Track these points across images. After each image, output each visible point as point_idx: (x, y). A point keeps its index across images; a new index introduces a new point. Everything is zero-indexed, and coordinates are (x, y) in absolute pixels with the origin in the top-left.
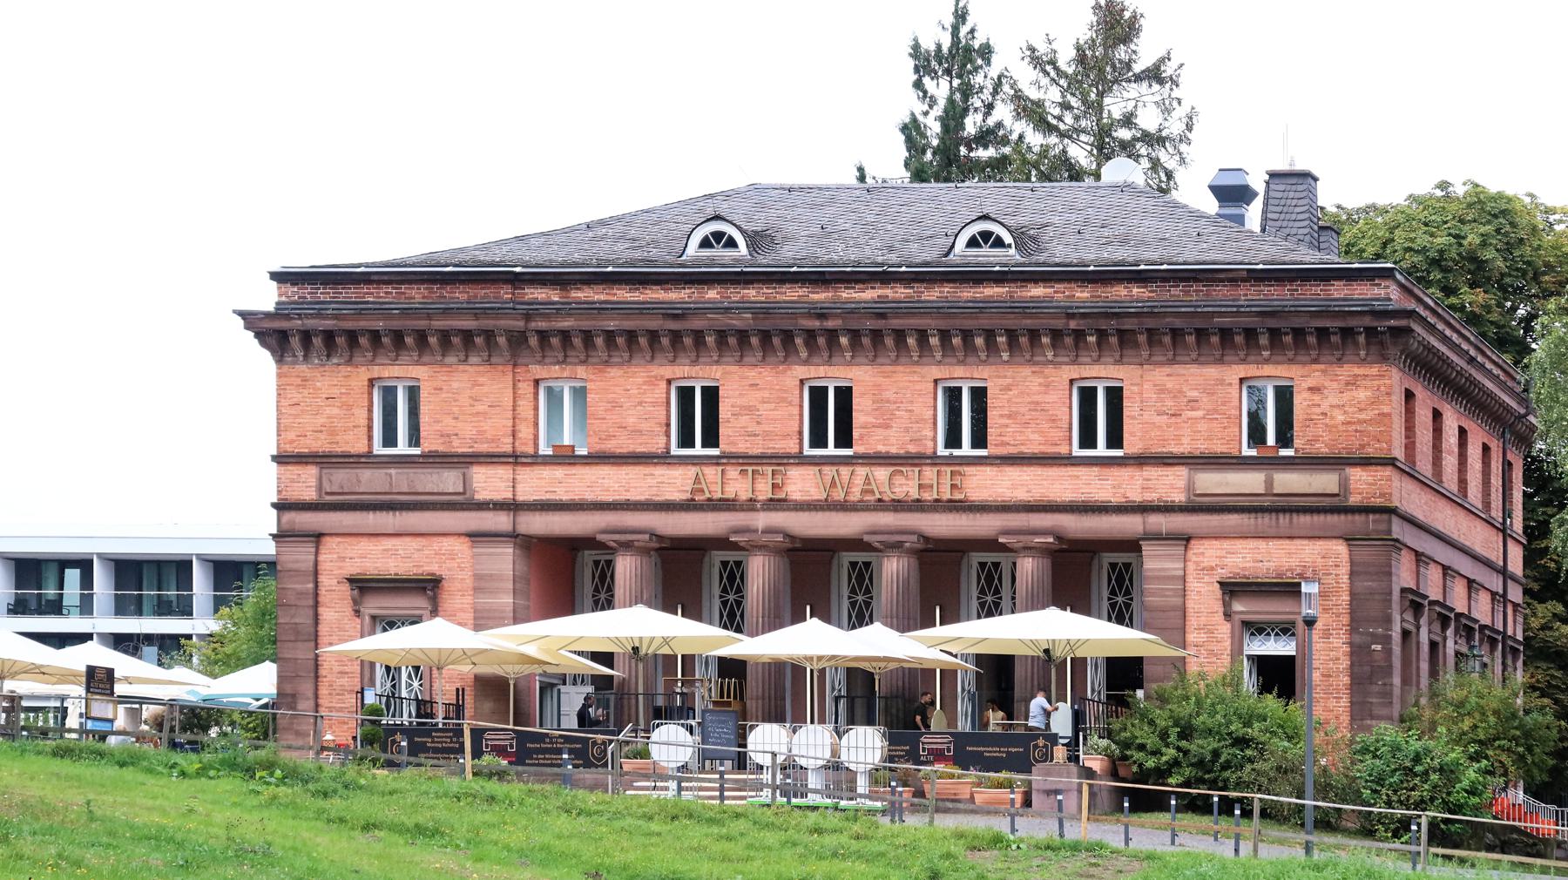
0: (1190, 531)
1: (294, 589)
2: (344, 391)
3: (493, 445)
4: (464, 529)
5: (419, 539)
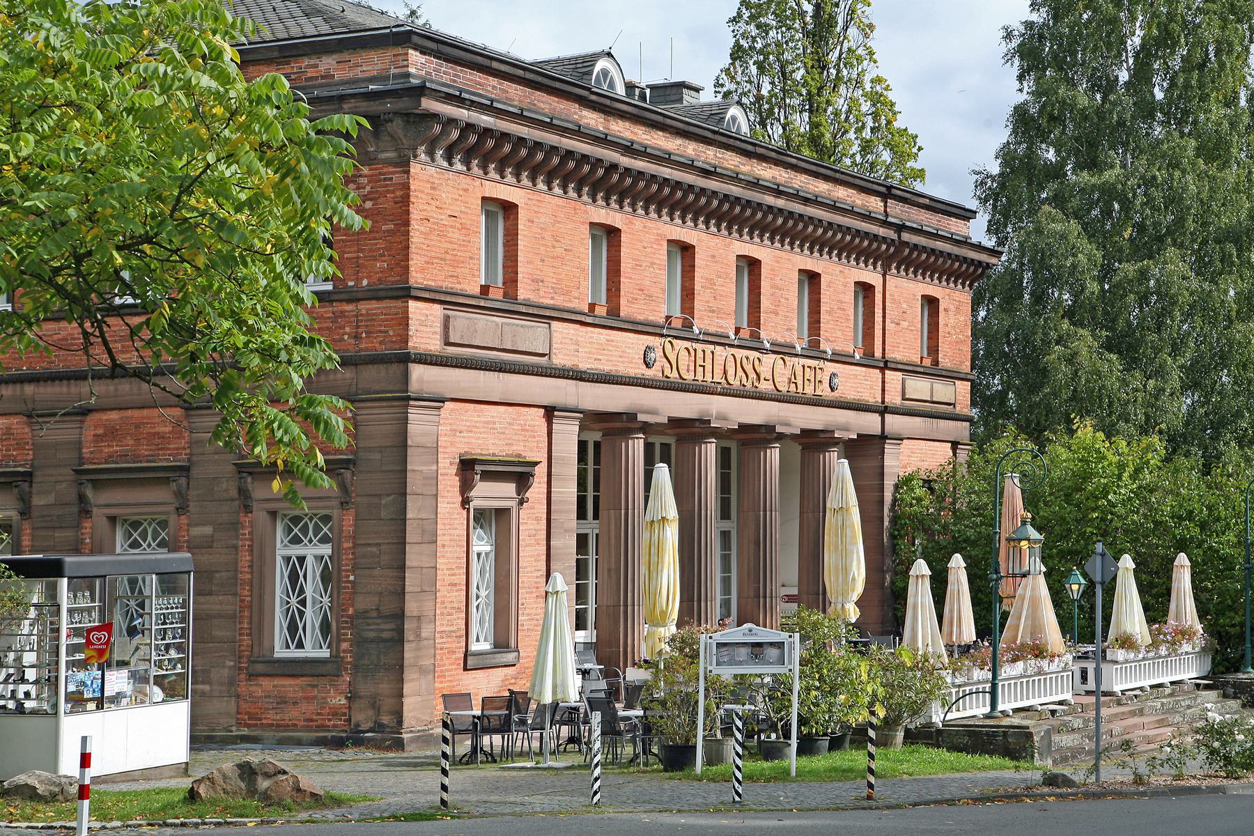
0: (901, 432)
1: (422, 471)
2: (463, 209)
3: (567, 298)
4: (546, 402)
5: (510, 409)
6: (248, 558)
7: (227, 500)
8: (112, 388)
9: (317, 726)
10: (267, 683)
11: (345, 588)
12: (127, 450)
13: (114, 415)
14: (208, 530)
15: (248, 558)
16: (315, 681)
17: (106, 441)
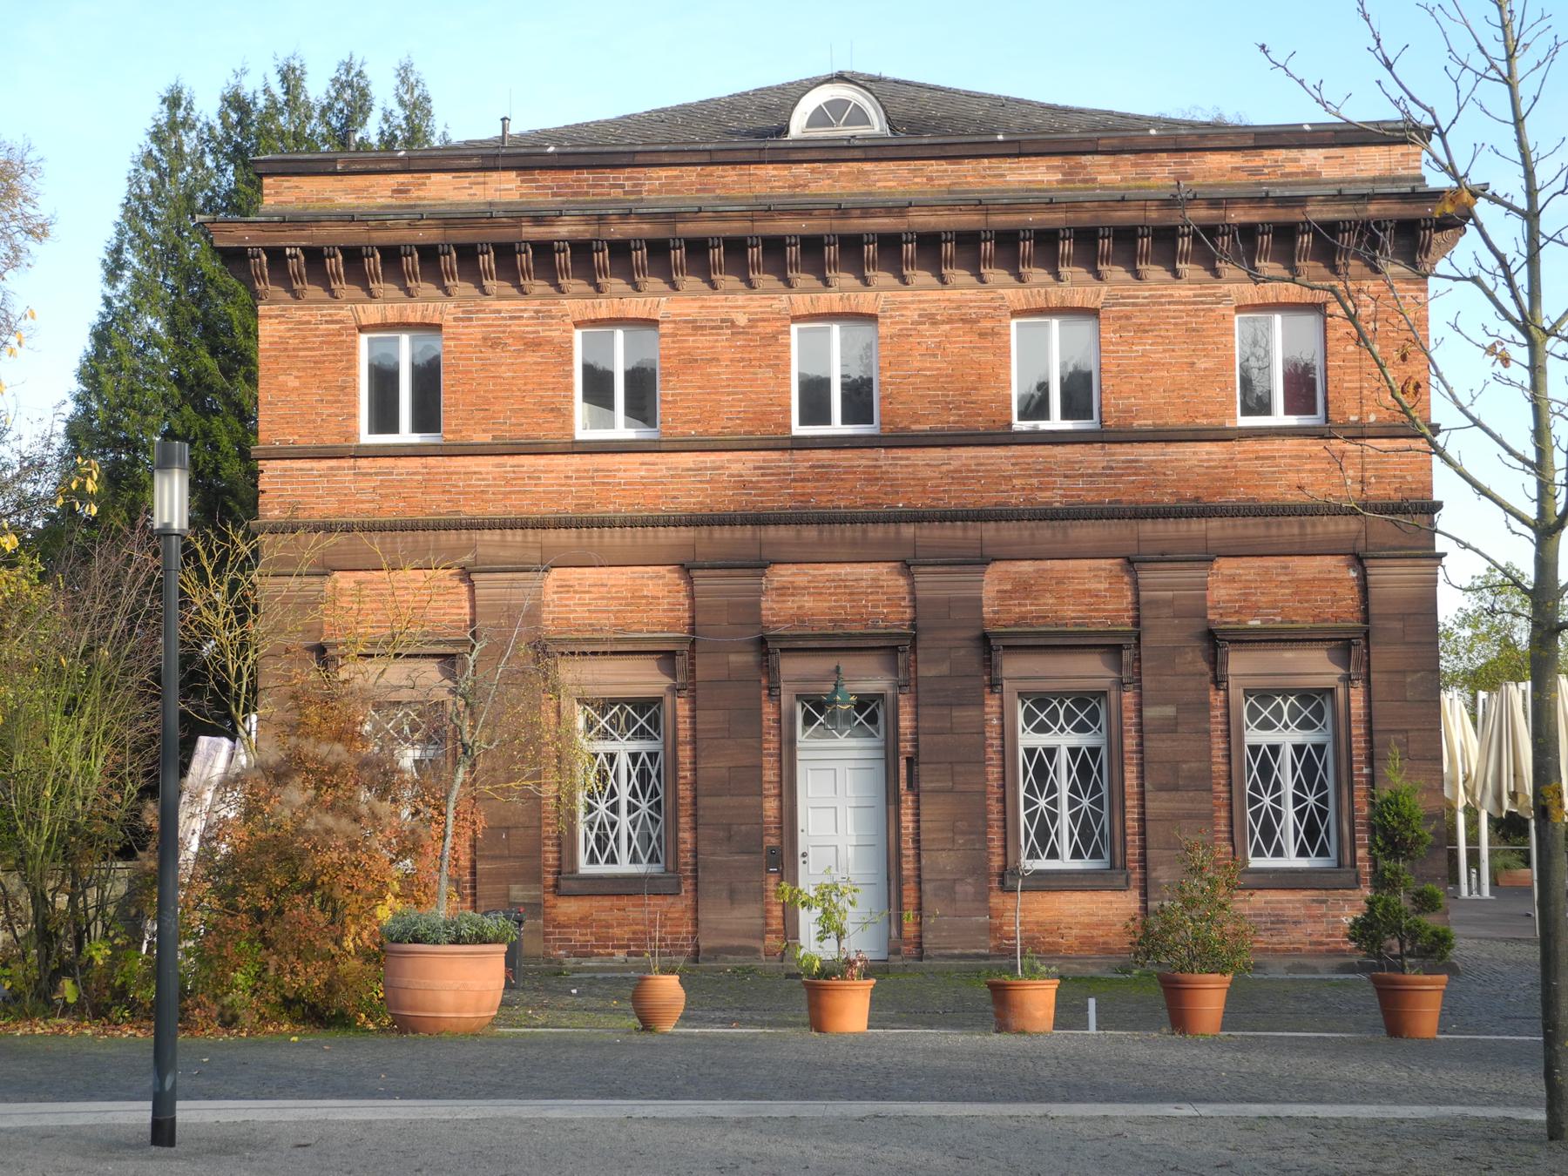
6: (1223, 746)
7: (1195, 674)
8: (1026, 533)
9: (1329, 951)
10: (1261, 898)
11: (1358, 783)
12: (1047, 611)
13: (1026, 567)
14: (1170, 711)
15: (1223, 746)
16: (1322, 895)
17: (1016, 599)
